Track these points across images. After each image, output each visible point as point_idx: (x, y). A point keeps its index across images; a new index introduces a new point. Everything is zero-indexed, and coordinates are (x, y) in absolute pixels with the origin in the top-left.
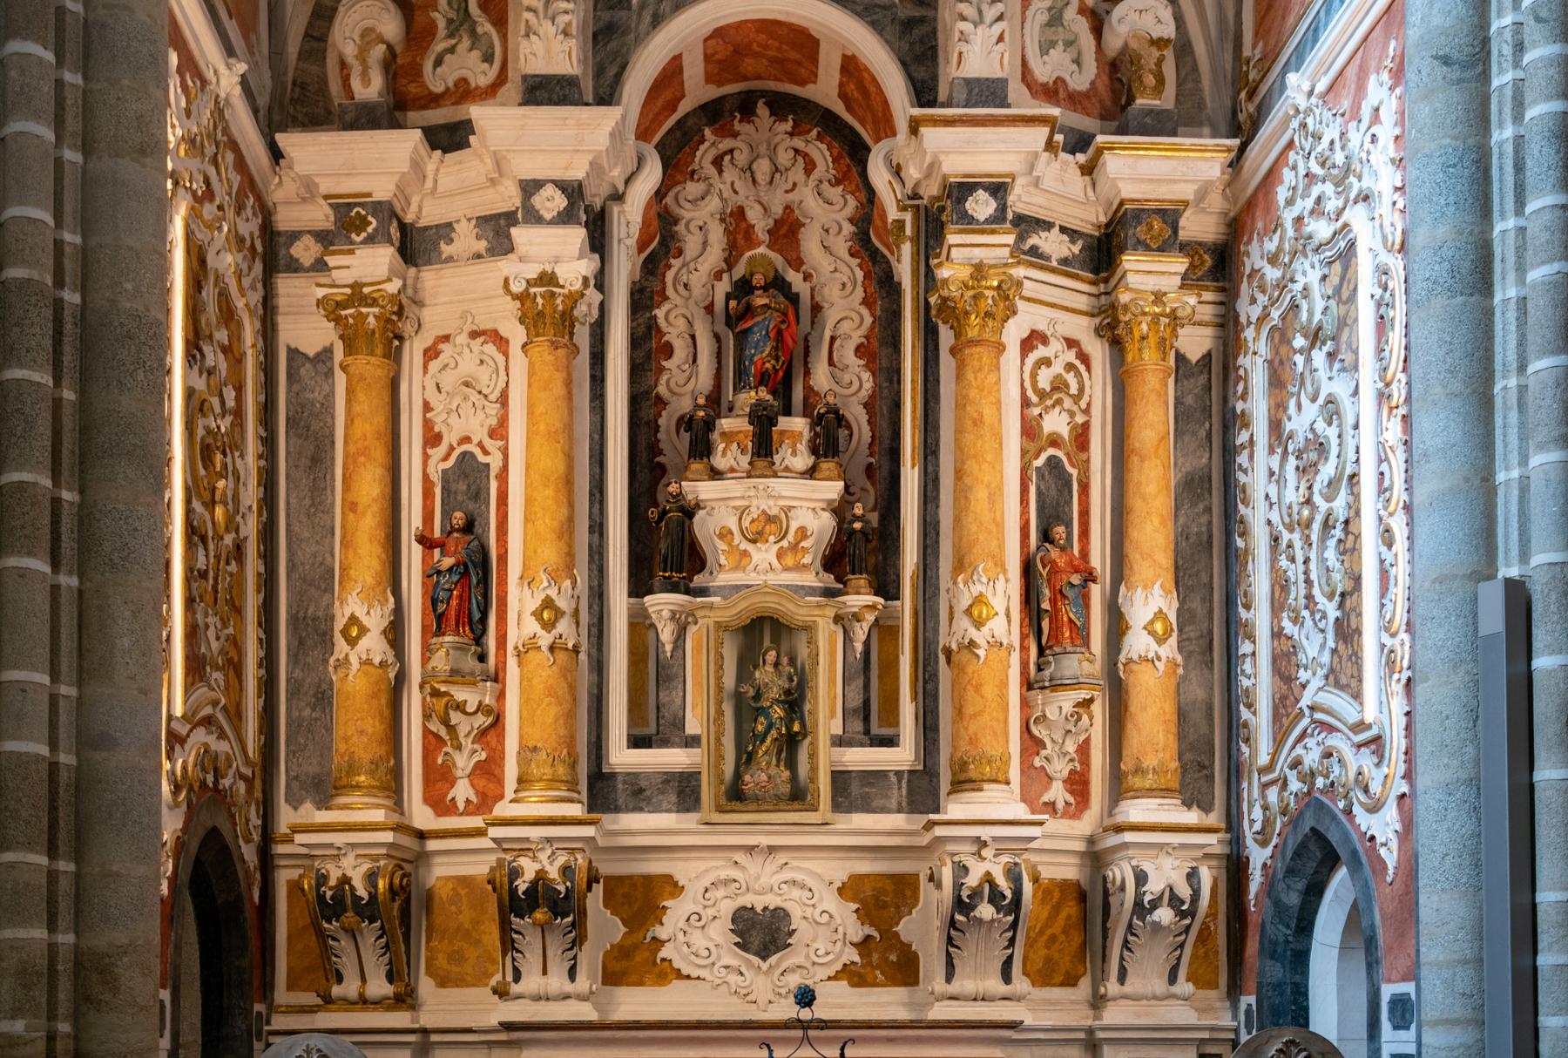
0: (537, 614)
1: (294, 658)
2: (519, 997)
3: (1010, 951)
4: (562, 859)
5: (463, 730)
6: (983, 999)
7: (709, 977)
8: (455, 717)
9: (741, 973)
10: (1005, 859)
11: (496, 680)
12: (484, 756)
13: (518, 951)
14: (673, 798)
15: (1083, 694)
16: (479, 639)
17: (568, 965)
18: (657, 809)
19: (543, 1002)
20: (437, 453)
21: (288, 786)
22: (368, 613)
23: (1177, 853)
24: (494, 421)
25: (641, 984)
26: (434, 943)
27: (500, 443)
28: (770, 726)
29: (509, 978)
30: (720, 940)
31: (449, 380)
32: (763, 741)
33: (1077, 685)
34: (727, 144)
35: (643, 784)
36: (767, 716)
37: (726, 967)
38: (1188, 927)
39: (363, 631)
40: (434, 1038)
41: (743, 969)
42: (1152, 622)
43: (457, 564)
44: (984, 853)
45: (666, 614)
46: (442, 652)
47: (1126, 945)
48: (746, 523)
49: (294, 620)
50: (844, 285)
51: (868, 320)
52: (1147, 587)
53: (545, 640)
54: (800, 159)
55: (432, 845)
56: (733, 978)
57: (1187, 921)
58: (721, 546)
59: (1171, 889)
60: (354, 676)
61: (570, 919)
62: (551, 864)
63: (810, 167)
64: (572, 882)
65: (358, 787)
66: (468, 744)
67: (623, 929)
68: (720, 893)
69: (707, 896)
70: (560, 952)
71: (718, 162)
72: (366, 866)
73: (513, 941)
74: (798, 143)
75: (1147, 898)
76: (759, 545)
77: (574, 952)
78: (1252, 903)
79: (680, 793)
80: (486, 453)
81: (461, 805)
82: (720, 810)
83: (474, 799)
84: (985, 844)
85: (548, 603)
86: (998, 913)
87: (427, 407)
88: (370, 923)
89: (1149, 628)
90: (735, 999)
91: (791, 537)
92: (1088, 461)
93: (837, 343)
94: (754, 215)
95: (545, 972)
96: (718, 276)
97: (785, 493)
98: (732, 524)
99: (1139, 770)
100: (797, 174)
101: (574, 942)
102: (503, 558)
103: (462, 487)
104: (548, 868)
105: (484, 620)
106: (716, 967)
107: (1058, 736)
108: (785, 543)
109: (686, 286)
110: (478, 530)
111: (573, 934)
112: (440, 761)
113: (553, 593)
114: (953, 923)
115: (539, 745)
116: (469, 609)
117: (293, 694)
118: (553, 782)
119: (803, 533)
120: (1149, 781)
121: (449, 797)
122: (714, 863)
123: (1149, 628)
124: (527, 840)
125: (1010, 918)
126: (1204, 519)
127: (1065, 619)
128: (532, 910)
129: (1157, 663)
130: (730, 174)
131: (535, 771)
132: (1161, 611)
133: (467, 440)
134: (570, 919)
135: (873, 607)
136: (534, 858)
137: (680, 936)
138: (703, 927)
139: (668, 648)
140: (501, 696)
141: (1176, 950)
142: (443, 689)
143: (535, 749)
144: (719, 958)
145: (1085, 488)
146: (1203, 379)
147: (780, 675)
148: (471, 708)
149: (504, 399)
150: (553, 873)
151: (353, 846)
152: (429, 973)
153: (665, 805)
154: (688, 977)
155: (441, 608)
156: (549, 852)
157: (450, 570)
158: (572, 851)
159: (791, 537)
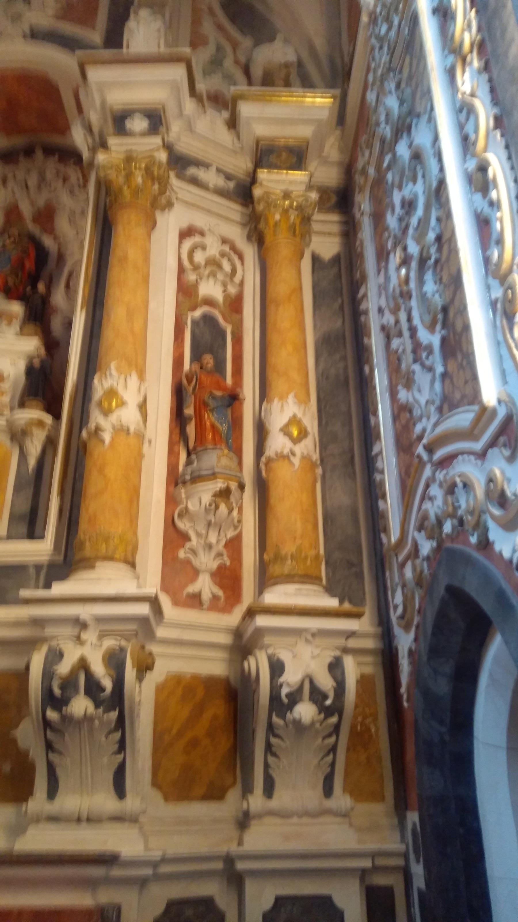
3: (120, 757)
6: (89, 820)
10: (109, 643)
15: (219, 485)
23: (318, 641)
33: (213, 476)
38: (337, 728)
42: (287, 425)
44: (84, 636)
47: (269, 748)
52: (283, 398)
57: (334, 720)
59: (311, 682)
75: (285, 691)
78: (405, 697)
84: (83, 626)
86: (97, 706)
89: (285, 431)
92: (241, 321)
99: (278, 558)
107: (202, 528)
114: (47, 724)
120: (288, 567)
123: (285, 431)
125: (114, 715)
126: (341, 365)
127: (208, 424)
129: (292, 458)
132: (295, 416)
135: (40, 424)
141: (328, 754)
145: (238, 341)
146: (335, 270)
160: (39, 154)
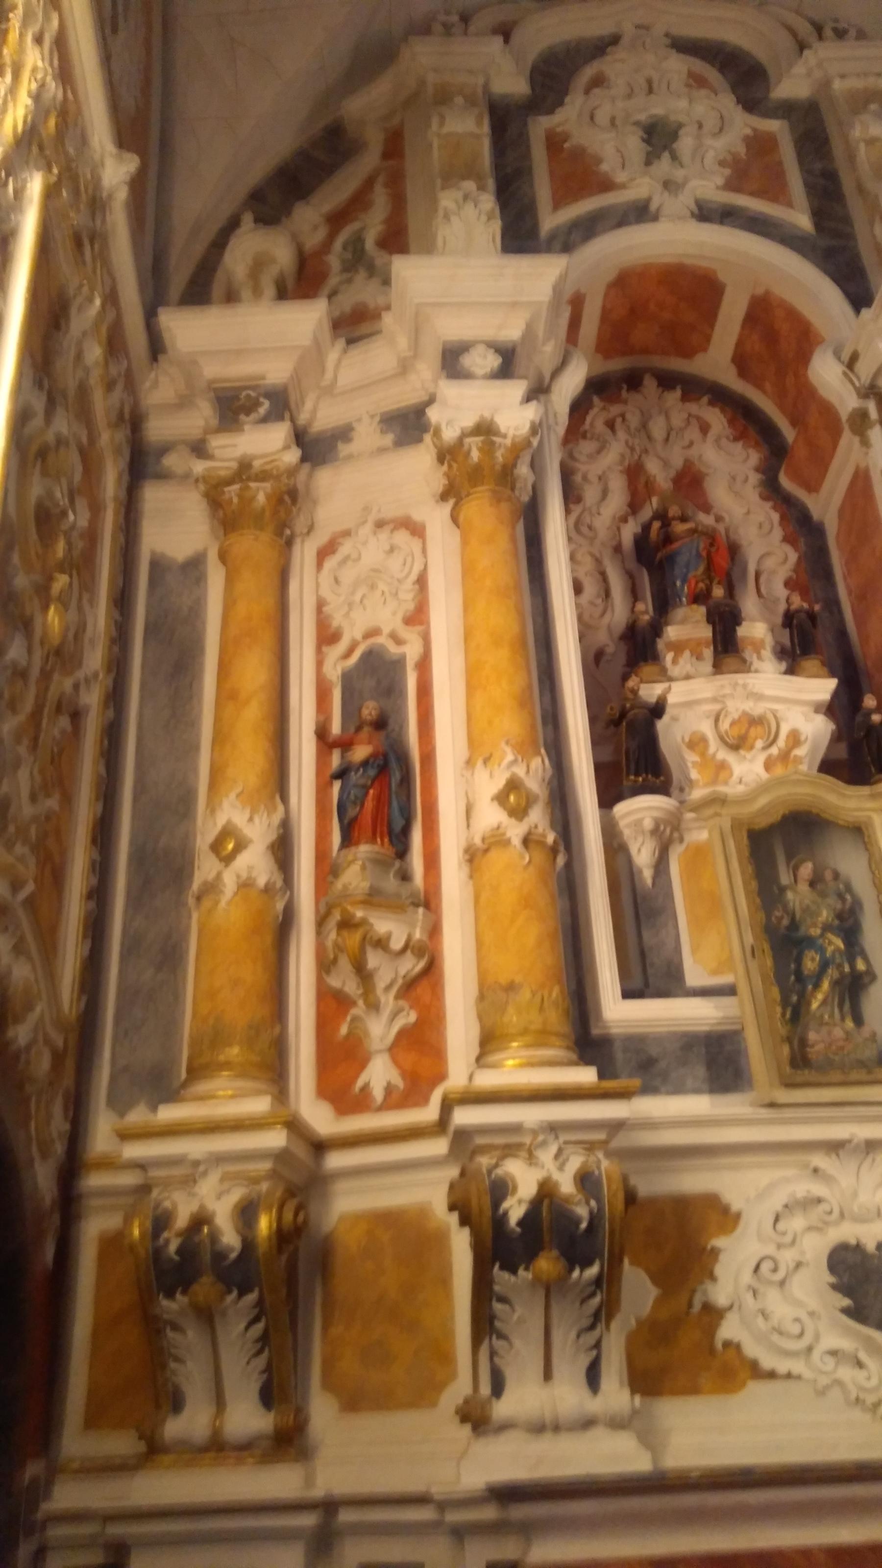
0: (501, 798)
1: (134, 902)
2: (505, 1427)
4: (575, 1163)
5: (382, 980)
7: (807, 1374)
8: (373, 960)
9: (860, 1365)
11: (427, 905)
12: (413, 1017)
13: (501, 1336)
14: (701, 1071)
16: (402, 852)
17: (584, 1361)
18: (679, 1090)
19: (548, 1436)
20: (334, 652)
21: (113, 1079)
22: (251, 819)
24: (411, 606)
25: (693, 1390)
26: (336, 1330)
27: (419, 628)
28: (824, 966)
29: (485, 1389)
30: (813, 1304)
31: (348, 575)
32: (817, 986)
34: (615, 410)
35: (654, 1051)
36: (822, 950)
37: (834, 1353)
39: (240, 846)
40: (346, 1516)
41: (863, 1356)
43: (374, 755)
45: (648, 824)
46: (356, 868)
48: (725, 725)
49: (138, 858)
50: (760, 526)
51: (793, 556)
53: (515, 831)
54: (694, 422)
55: (335, 1160)
56: (846, 1373)
58: (691, 757)
60: (229, 903)
61: (593, 1271)
62: (561, 1168)
63: (705, 428)
64: (599, 1201)
65: (227, 1065)
66: (388, 1001)
67: (653, 1292)
68: (796, 1223)
69: (781, 1226)
70: (573, 1334)
71: (611, 425)
72: (236, 1195)
73: (492, 1318)
74: (692, 408)
76: (742, 752)
77: (596, 1333)
79: (711, 1064)
80: (399, 642)
81: (378, 1094)
82: (790, 1085)
83: (399, 1082)
85: (513, 785)
87: (320, 605)
88: (241, 1295)
90: (857, 1414)
91: (781, 742)
93: (762, 579)
94: (653, 467)
95: (548, 1375)
96: (624, 520)
97: (768, 692)
98: (706, 728)
100: (693, 433)
101: (596, 1316)
102: (429, 758)
103: (370, 683)
104: (556, 1176)
105: (406, 831)
106: (816, 1354)
108: (774, 751)
109: (590, 527)
110: (392, 724)
111: (597, 1300)
112: (344, 1030)
113: (520, 771)
115: (518, 979)
116: (389, 815)
117: (130, 949)
118: (541, 1038)
119: (795, 738)
121: (360, 1083)
122: (779, 1174)
124: (516, 1129)
128: (530, 1256)
130: (621, 434)
131: (512, 1018)
133: (374, 632)
134: (593, 1271)
136: (531, 1159)
137: (749, 1298)
138: (782, 1283)
139: (647, 875)
140: (435, 930)
142: (359, 914)
143: (511, 987)
144: (817, 1337)
147: (823, 895)
148: (397, 944)
149: (422, 582)
150: (566, 1185)
151: (220, 1159)
152: (328, 1384)
153: (689, 1083)
154: (772, 1375)
155: (352, 812)
156: (553, 1149)
157: (365, 764)
158: (590, 1147)
159: (781, 742)
160: (650, 384)
